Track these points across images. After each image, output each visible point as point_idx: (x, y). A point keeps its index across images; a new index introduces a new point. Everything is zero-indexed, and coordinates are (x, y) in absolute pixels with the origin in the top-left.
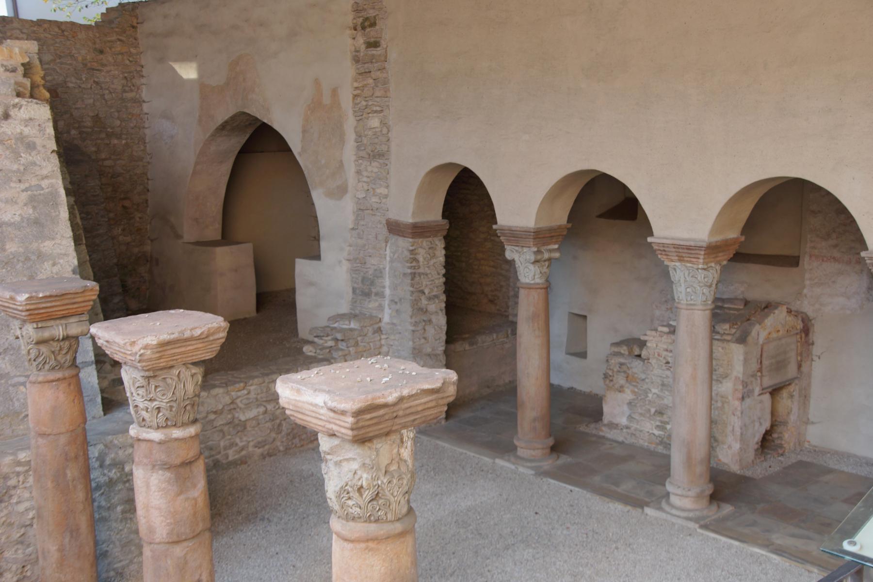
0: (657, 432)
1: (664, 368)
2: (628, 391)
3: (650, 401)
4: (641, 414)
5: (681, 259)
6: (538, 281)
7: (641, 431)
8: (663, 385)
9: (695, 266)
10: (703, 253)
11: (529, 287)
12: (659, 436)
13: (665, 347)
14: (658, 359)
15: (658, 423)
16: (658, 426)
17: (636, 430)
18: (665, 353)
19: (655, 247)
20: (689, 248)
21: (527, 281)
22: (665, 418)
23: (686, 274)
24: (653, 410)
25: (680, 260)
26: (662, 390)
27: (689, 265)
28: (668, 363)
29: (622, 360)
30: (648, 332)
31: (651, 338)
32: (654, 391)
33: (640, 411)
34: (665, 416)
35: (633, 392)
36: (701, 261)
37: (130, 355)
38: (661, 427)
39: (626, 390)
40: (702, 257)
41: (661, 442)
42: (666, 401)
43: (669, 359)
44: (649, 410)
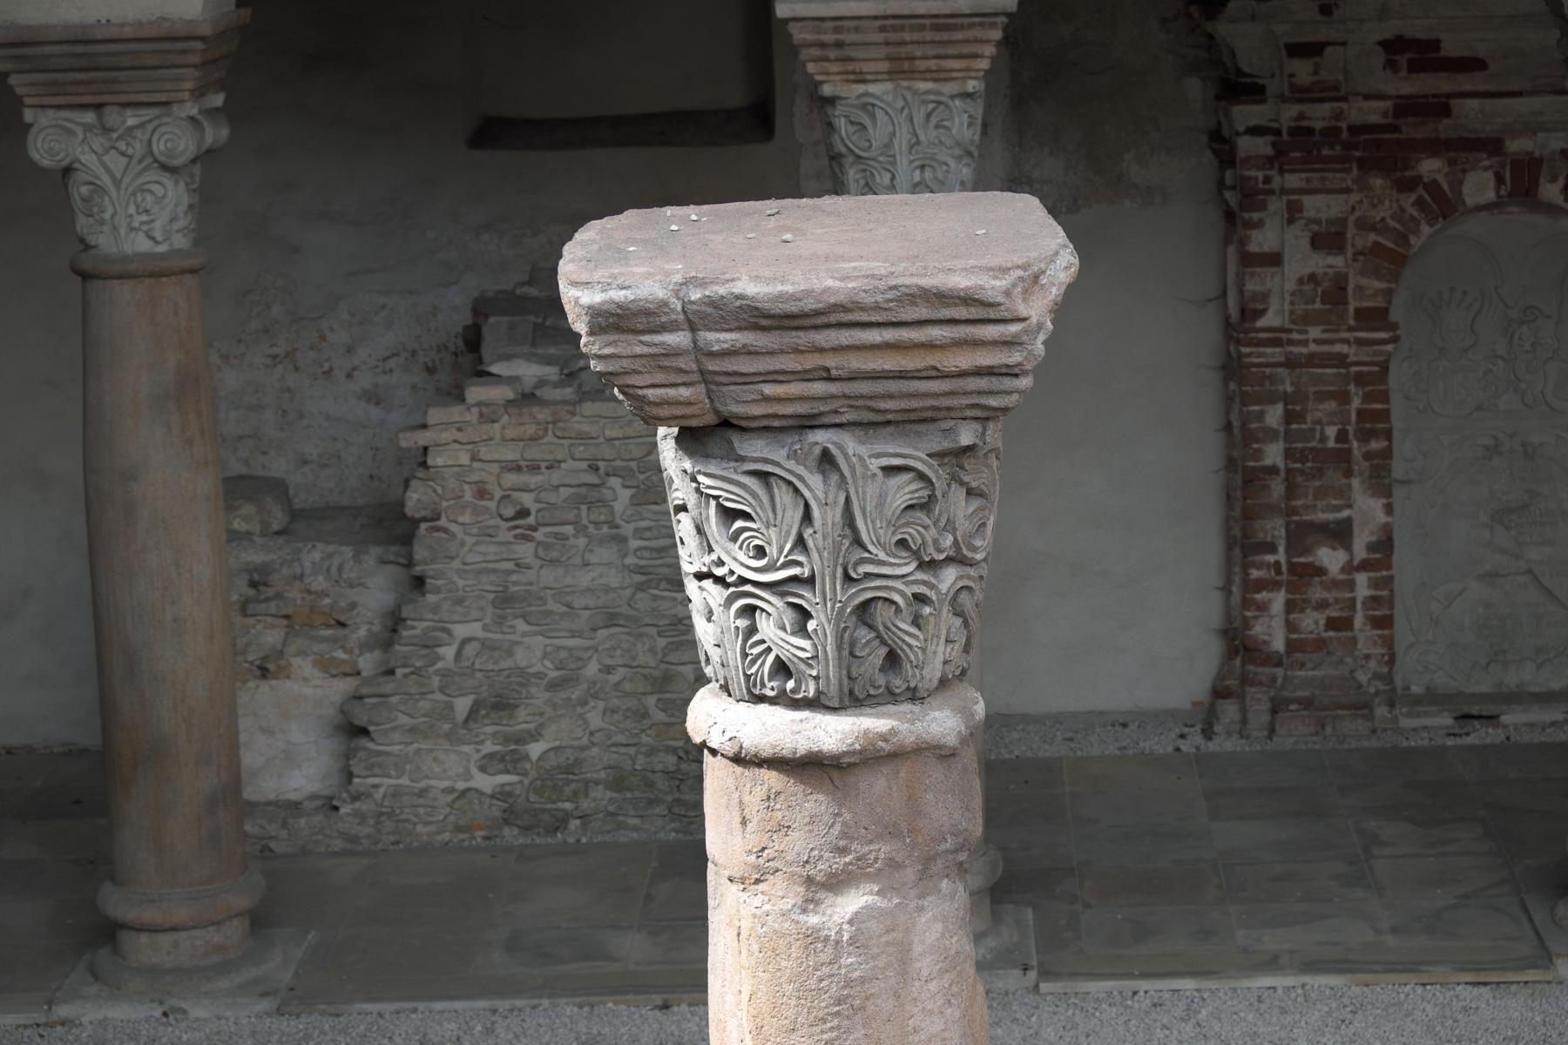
0: (486, 783)
1: (505, 535)
2: (303, 666)
3: (445, 674)
4: (413, 730)
5: (901, 68)
6: (180, 242)
7: (423, 793)
8: (504, 600)
9: (949, 88)
10: (997, 35)
11: (154, 271)
12: (502, 794)
13: (510, 455)
14: (476, 511)
15: (489, 747)
16: (491, 756)
17: (396, 793)
18: (511, 479)
19: (799, 34)
20: (945, 22)
21: (143, 245)
22: (523, 720)
23: (919, 118)
24: (462, 705)
25: (893, 75)
26: (500, 620)
27: (923, 86)
28: (523, 513)
29: (255, 557)
30: (435, 415)
31: (446, 436)
32: (461, 631)
33: (404, 720)
34: (521, 713)
35: (328, 667)
36: (984, 64)
37: (1009, 343)
38: (508, 760)
39: (297, 662)
40: (989, 50)
41: (509, 816)
42: (520, 658)
43: (527, 500)
44: (450, 707)
